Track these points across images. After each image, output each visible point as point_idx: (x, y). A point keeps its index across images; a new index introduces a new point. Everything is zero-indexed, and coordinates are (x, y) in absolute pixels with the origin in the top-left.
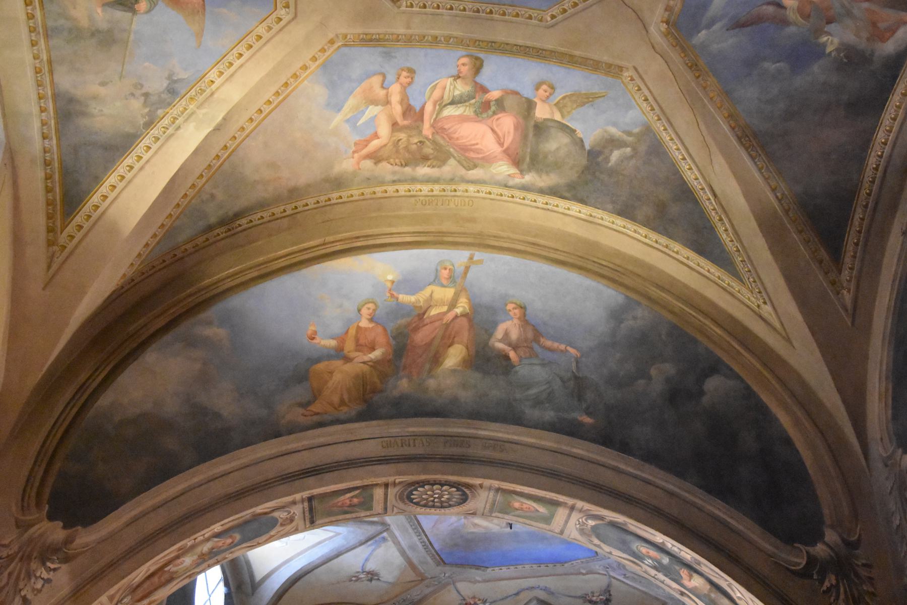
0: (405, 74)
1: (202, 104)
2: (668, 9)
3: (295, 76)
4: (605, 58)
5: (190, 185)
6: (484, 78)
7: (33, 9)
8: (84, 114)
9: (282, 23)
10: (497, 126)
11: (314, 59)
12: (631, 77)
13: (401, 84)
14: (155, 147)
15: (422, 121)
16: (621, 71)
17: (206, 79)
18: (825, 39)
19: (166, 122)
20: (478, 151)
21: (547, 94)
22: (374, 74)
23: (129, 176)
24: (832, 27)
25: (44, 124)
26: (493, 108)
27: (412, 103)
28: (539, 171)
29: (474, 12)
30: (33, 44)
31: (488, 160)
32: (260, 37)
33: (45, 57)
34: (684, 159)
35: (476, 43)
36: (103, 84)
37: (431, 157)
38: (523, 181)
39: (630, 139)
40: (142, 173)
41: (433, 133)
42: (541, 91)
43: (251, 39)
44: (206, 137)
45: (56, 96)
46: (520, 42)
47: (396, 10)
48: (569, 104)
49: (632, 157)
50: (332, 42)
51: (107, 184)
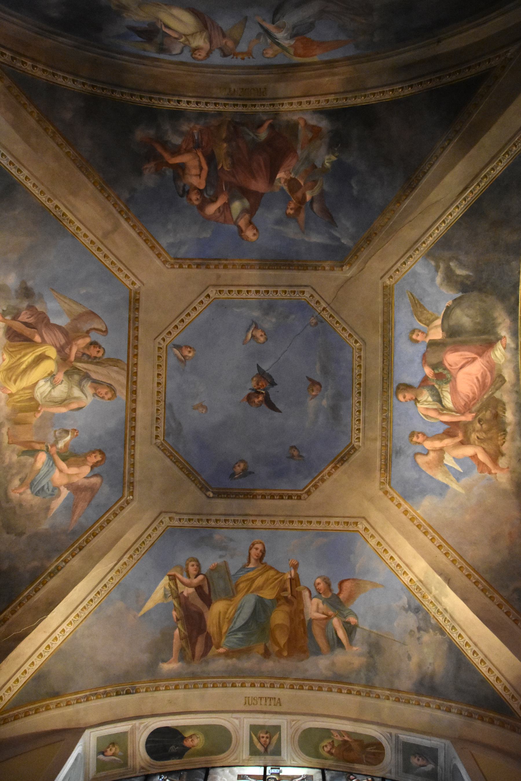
0: (415, 439)
1: (428, 589)
2: (332, 269)
3: (412, 519)
4: (380, 299)
5: (498, 609)
6: (415, 381)
7: (354, 690)
8: (432, 677)
9: (368, 527)
10: (457, 365)
11: (399, 505)
12: (389, 278)
13: (424, 441)
14: (460, 631)
15: (459, 422)
16: (387, 286)
17: (409, 584)
18: (327, 164)
19: (441, 618)
20: (484, 376)
21: (420, 334)
22: (415, 461)
23: (481, 656)
24: (318, 164)
25: (439, 708)
26: (441, 370)
27: (441, 431)
28: (495, 326)
29: (360, 395)
30: (378, 697)
31: (492, 367)
32: (379, 543)
33: (388, 693)
34: (444, 222)
35: (385, 390)
36: (409, 658)
37: (494, 411)
38: (507, 337)
39: (442, 266)
40: (479, 645)
41: (470, 413)
42: (419, 338)
43: (380, 550)
44: (455, 591)
45: (418, 693)
46: (380, 360)
47: (362, 449)
48: (424, 316)
49: (457, 259)
50: (386, 493)
51: (487, 674)
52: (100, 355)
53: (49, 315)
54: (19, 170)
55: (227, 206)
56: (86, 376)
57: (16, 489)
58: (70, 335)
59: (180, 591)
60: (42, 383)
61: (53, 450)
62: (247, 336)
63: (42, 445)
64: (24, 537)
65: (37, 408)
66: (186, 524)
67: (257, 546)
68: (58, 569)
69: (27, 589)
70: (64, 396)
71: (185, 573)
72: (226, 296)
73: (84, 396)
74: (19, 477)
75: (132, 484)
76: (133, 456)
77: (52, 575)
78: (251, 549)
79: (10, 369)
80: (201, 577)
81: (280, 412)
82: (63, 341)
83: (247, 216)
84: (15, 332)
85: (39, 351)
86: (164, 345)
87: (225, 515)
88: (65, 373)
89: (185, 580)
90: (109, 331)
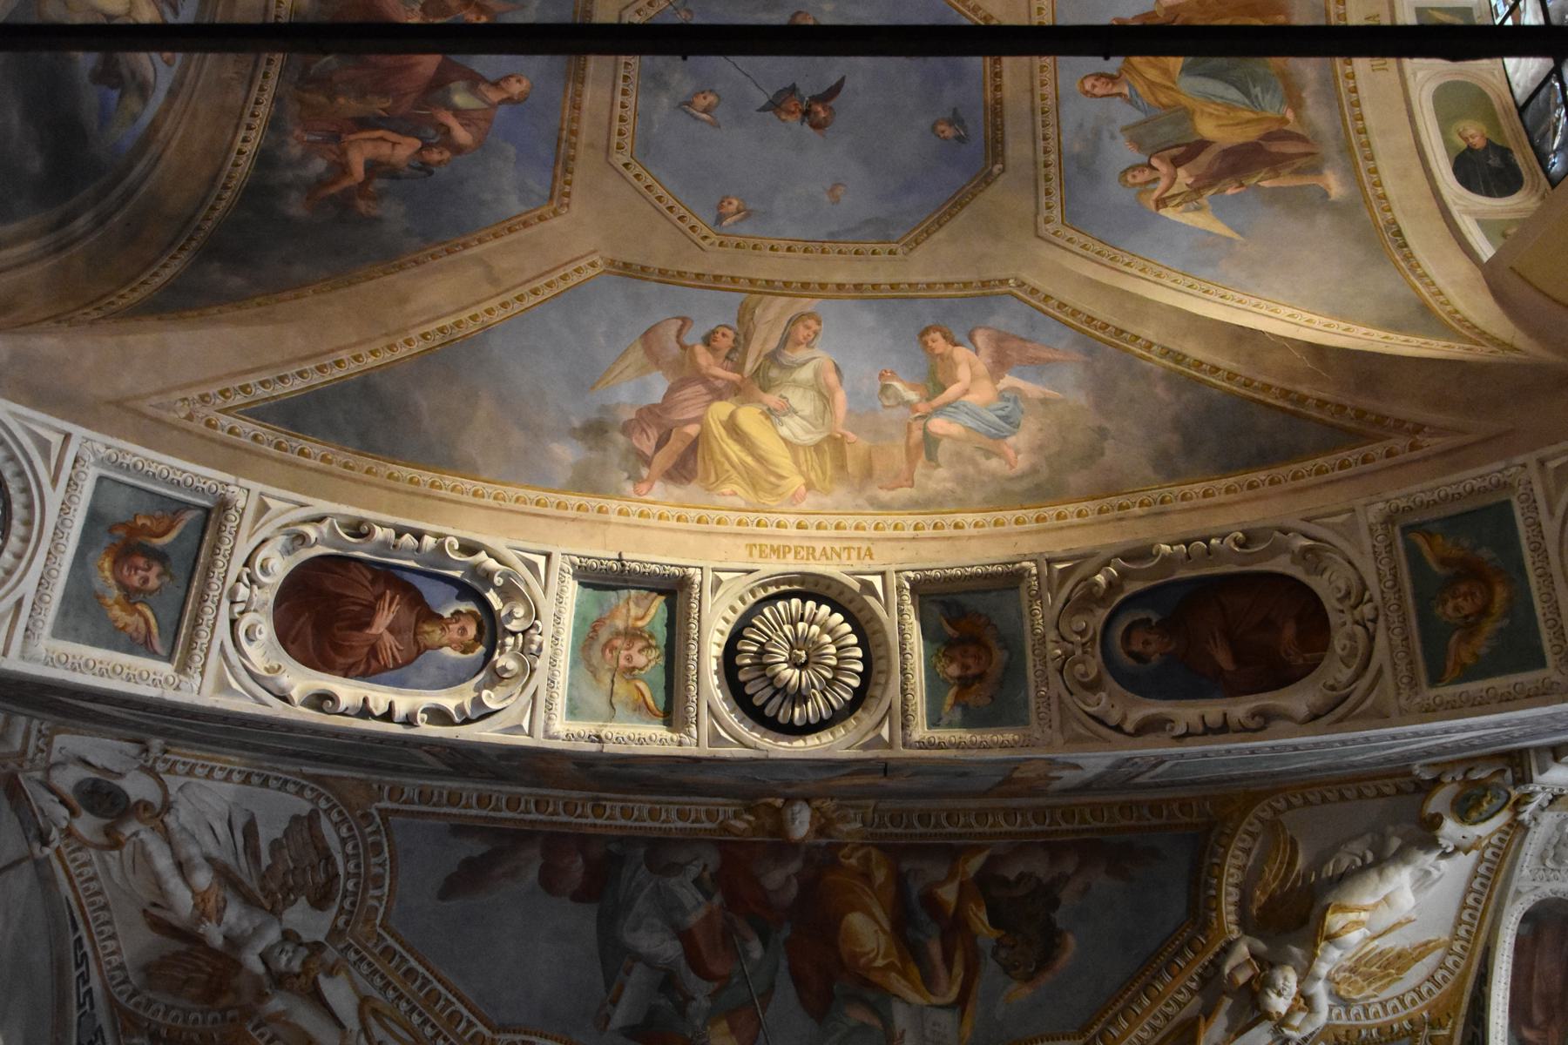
52: (730, 333)
53: (645, 403)
54: (338, 363)
55: (458, 112)
56: (773, 357)
57: (1008, 462)
58: (687, 375)
59: (1185, 188)
60: (784, 431)
61: (923, 408)
62: (703, 120)
63: (914, 427)
64: (1108, 425)
65: (836, 439)
66: (1056, 198)
67: (1088, 86)
68: (1167, 353)
69: (1216, 386)
70: (811, 394)
71: (1151, 186)
72: (629, 141)
73: (813, 362)
74: (981, 460)
75: (984, 284)
76: (929, 286)
77: (1179, 358)
78: (1095, 96)
79: (754, 483)
80: (1155, 162)
81: (843, 79)
82: (700, 388)
83: (483, 87)
84: (675, 466)
85: (718, 430)
86: (714, 238)
87: (1035, 142)
88: (765, 391)
89: (1162, 185)
90: (685, 314)
